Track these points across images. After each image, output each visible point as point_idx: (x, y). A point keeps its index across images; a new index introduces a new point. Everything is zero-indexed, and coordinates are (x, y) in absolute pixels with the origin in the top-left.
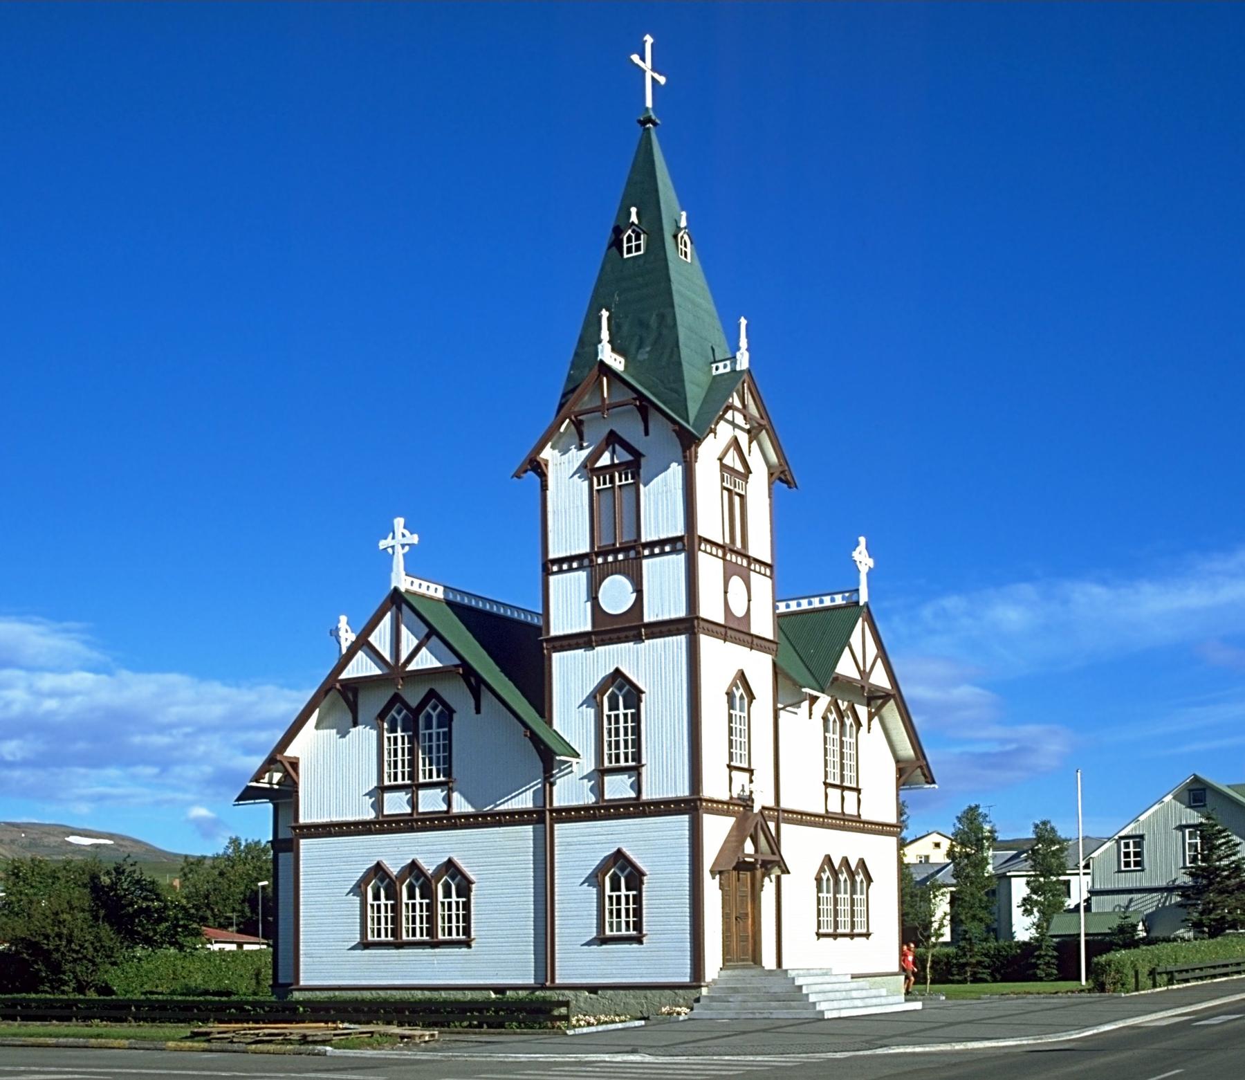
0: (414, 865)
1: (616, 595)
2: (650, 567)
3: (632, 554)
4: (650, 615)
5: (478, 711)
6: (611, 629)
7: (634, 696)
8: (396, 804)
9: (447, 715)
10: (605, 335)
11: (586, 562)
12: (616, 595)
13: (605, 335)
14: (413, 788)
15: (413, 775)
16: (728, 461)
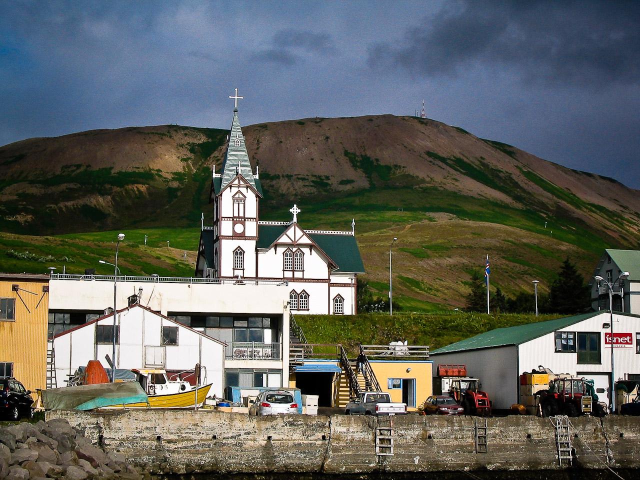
3: (243, 220)
6: (236, 236)
12: (239, 228)
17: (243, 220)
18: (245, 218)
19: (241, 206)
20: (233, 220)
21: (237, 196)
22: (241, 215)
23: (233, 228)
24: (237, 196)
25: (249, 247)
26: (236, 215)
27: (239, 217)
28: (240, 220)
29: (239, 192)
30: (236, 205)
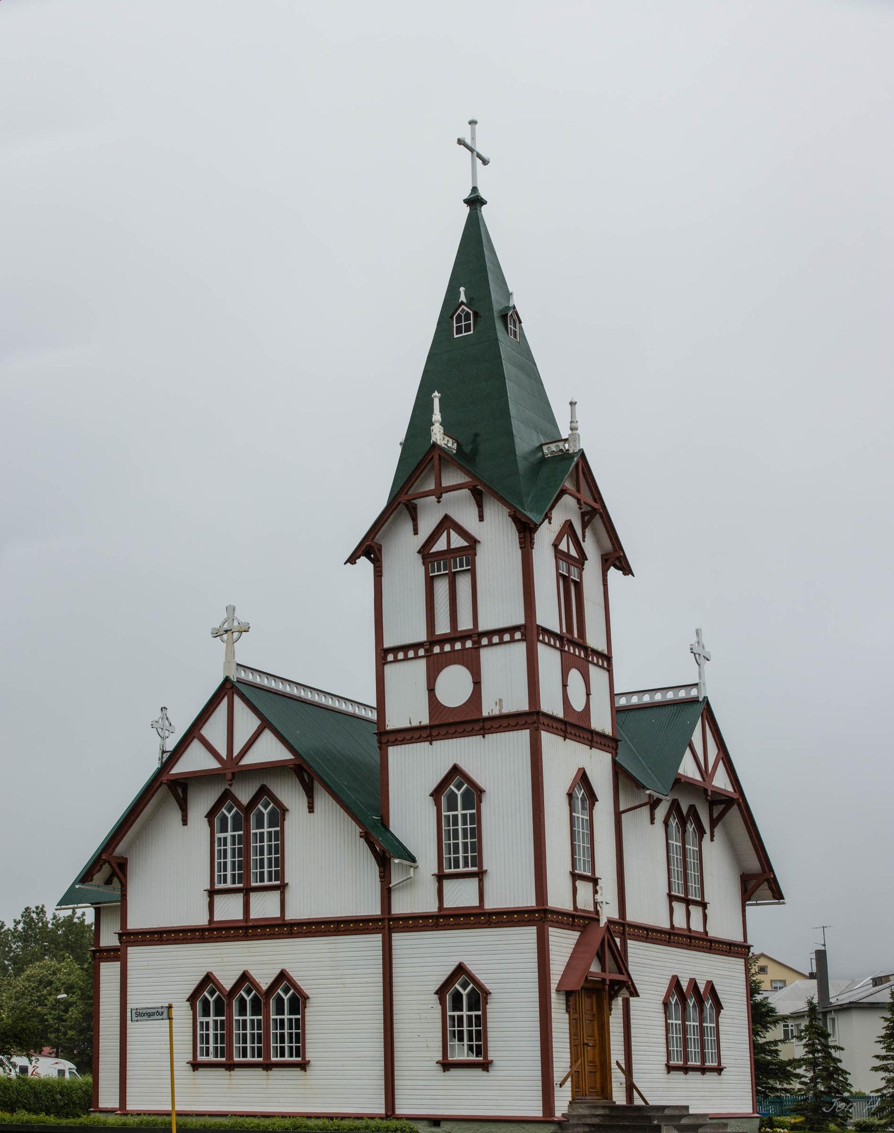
0: (245, 977)
1: (454, 686)
2: (490, 658)
3: (469, 644)
4: (488, 709)
5: (311, 809)
6: (445, 724)
7: (475, 795)
8: (229, 909)
9: (279, 815)
10: (437, 416)
11: (421, 652)
12: (454, 686)
13: (437, 416)
14: (247, 891)
15: (244, 877)
16: (563, 546)
17: (469, 644)
18: (476, 636)
19: (463, 584)
20: (429, 655)
21: (441, 545)
22: (465, 624)
23: (431, 690)
24: (441, 545)
25: (599, 766)
26: (443, 627)
27: (455, 636)
28: (447, 648)
29: (447, 524)
30: (442, 588)
